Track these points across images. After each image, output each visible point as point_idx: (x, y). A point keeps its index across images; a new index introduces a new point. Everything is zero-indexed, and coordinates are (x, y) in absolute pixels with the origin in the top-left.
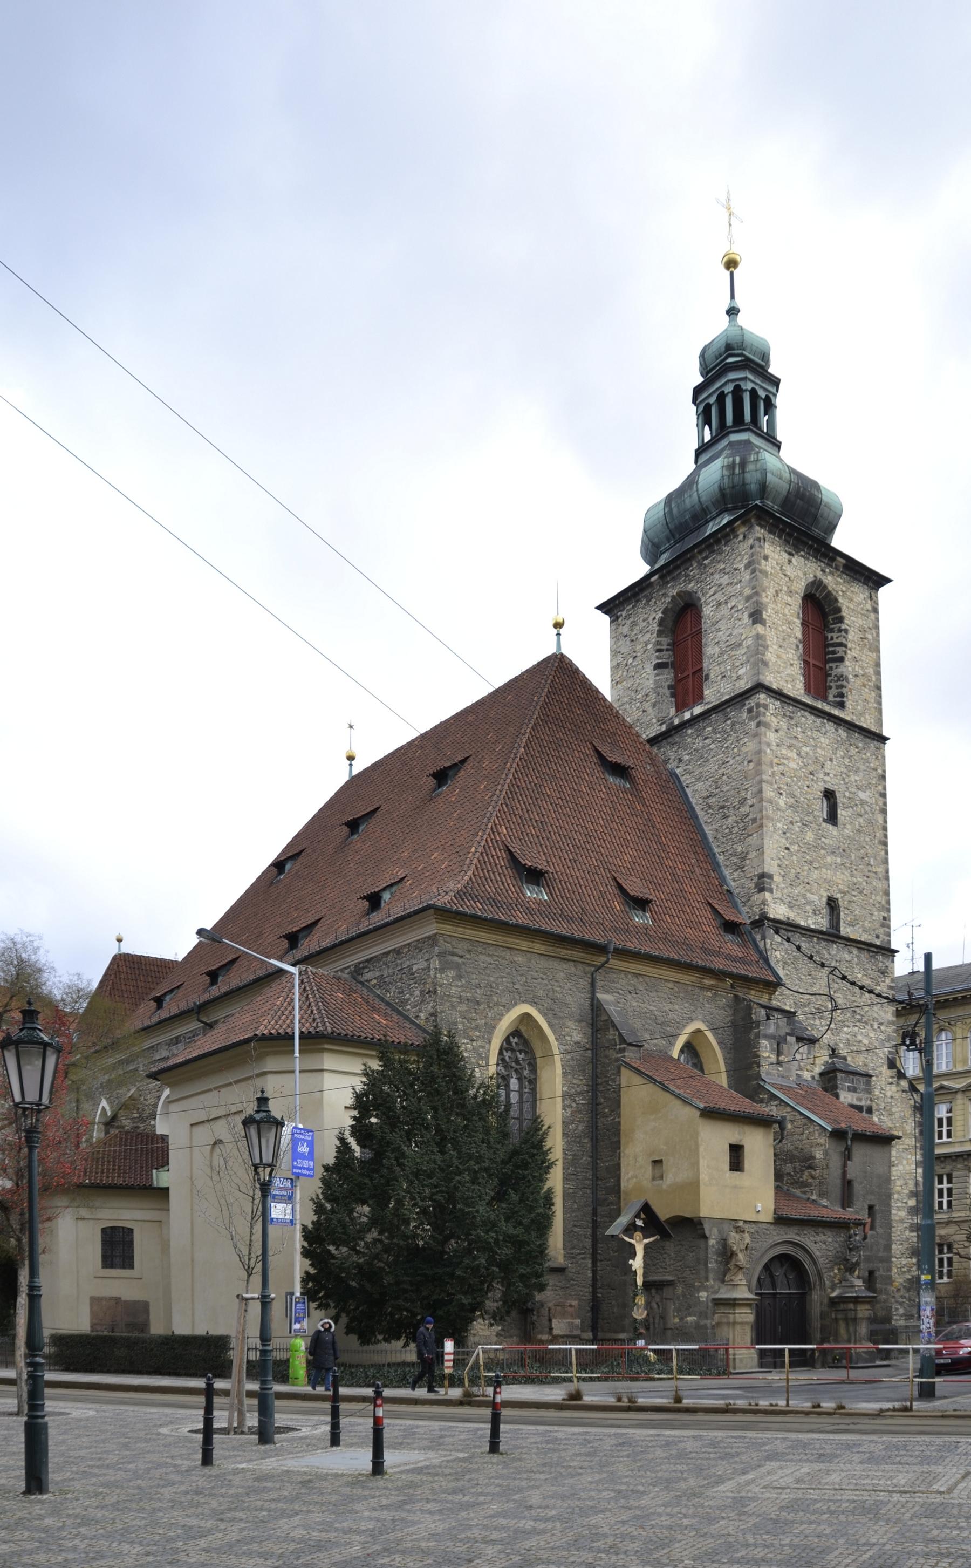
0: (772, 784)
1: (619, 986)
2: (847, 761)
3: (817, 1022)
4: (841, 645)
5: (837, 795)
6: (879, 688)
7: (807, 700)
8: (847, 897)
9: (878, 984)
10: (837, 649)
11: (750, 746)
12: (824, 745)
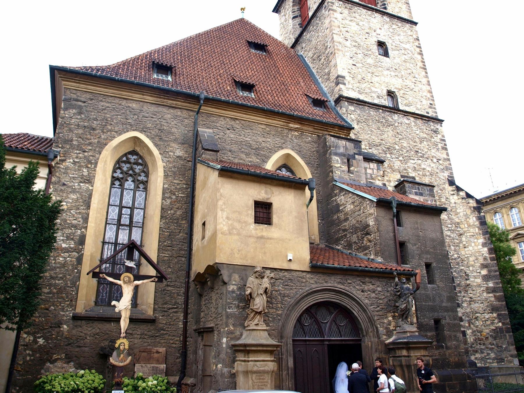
1: (218, 125)
2: (391, 30)
3: (388, 155)
5: (386, 43)
6: (408, 4)
7: (360, 2)
9: (432, 137)
11: (327, 21)
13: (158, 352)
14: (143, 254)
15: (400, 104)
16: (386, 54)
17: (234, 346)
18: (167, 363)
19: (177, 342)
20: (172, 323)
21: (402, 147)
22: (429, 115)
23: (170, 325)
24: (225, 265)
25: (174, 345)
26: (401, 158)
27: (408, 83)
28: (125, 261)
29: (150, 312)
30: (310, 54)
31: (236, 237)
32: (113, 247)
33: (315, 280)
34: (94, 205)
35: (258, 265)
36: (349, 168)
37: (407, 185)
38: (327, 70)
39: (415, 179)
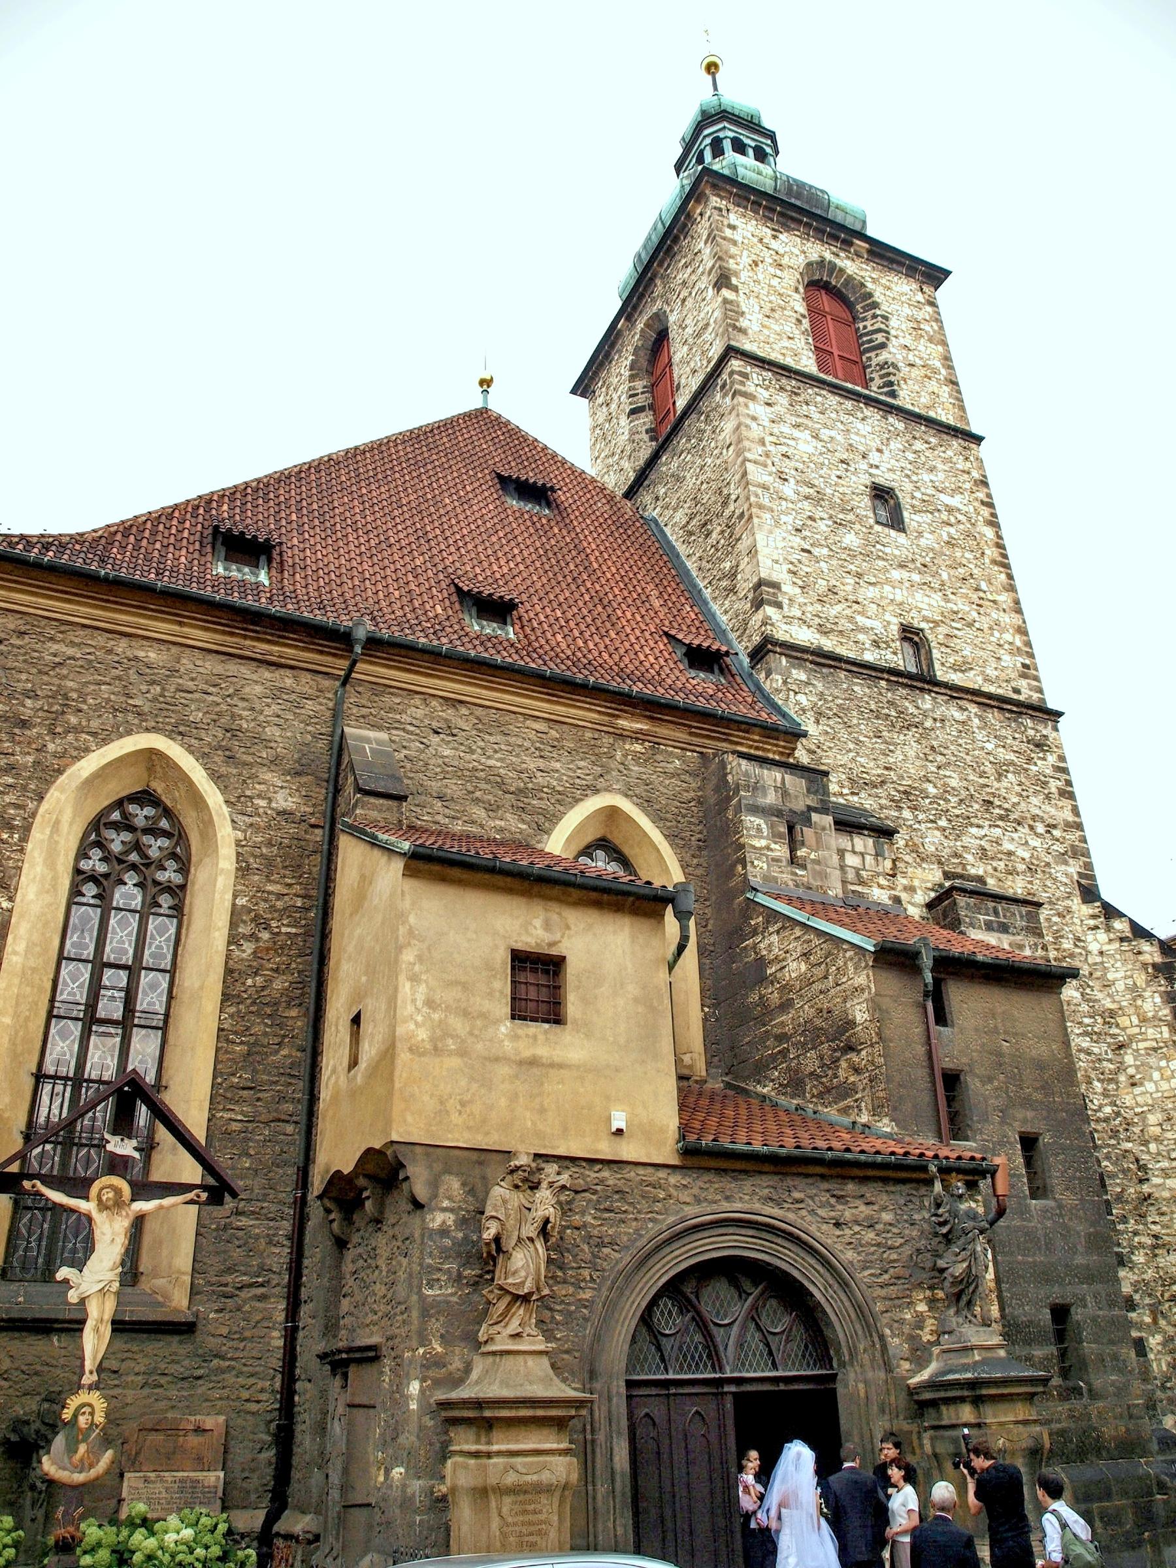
0: (766, 466)
1: (405, 718)
2: (911, 456)
3: (906, 814)
4: (879, 330)
7: (822, 375)
8: (943, 630)
9: (1029, 760)
10: (874, 336)
11: (728, 426)
12: (863, 432)
13: (199, 1430)
14: (162, 1114)
15: (937, 665)
16: (896, 522)
17: (445, 1405)
18: (229, 1464)
19: (264, 1397)
20: (247, 1334)
21: (947, 790)
22: (1022, 698)
23: (242, 1340)
24: (418, 1149)
25: (253, 1407)
26: (943, 823)
27: (961, 605)
28: (107, 1136)
29: (179, 1301)
30: (680, 517)
31: (455, 1062)
32: (69, 1089)
33: (696, 1191)
34: (15, 958)
35: (521, 1148)
36: (792, 850)
37: (962, 901)
38: (727, 565)
39: (985, 883)
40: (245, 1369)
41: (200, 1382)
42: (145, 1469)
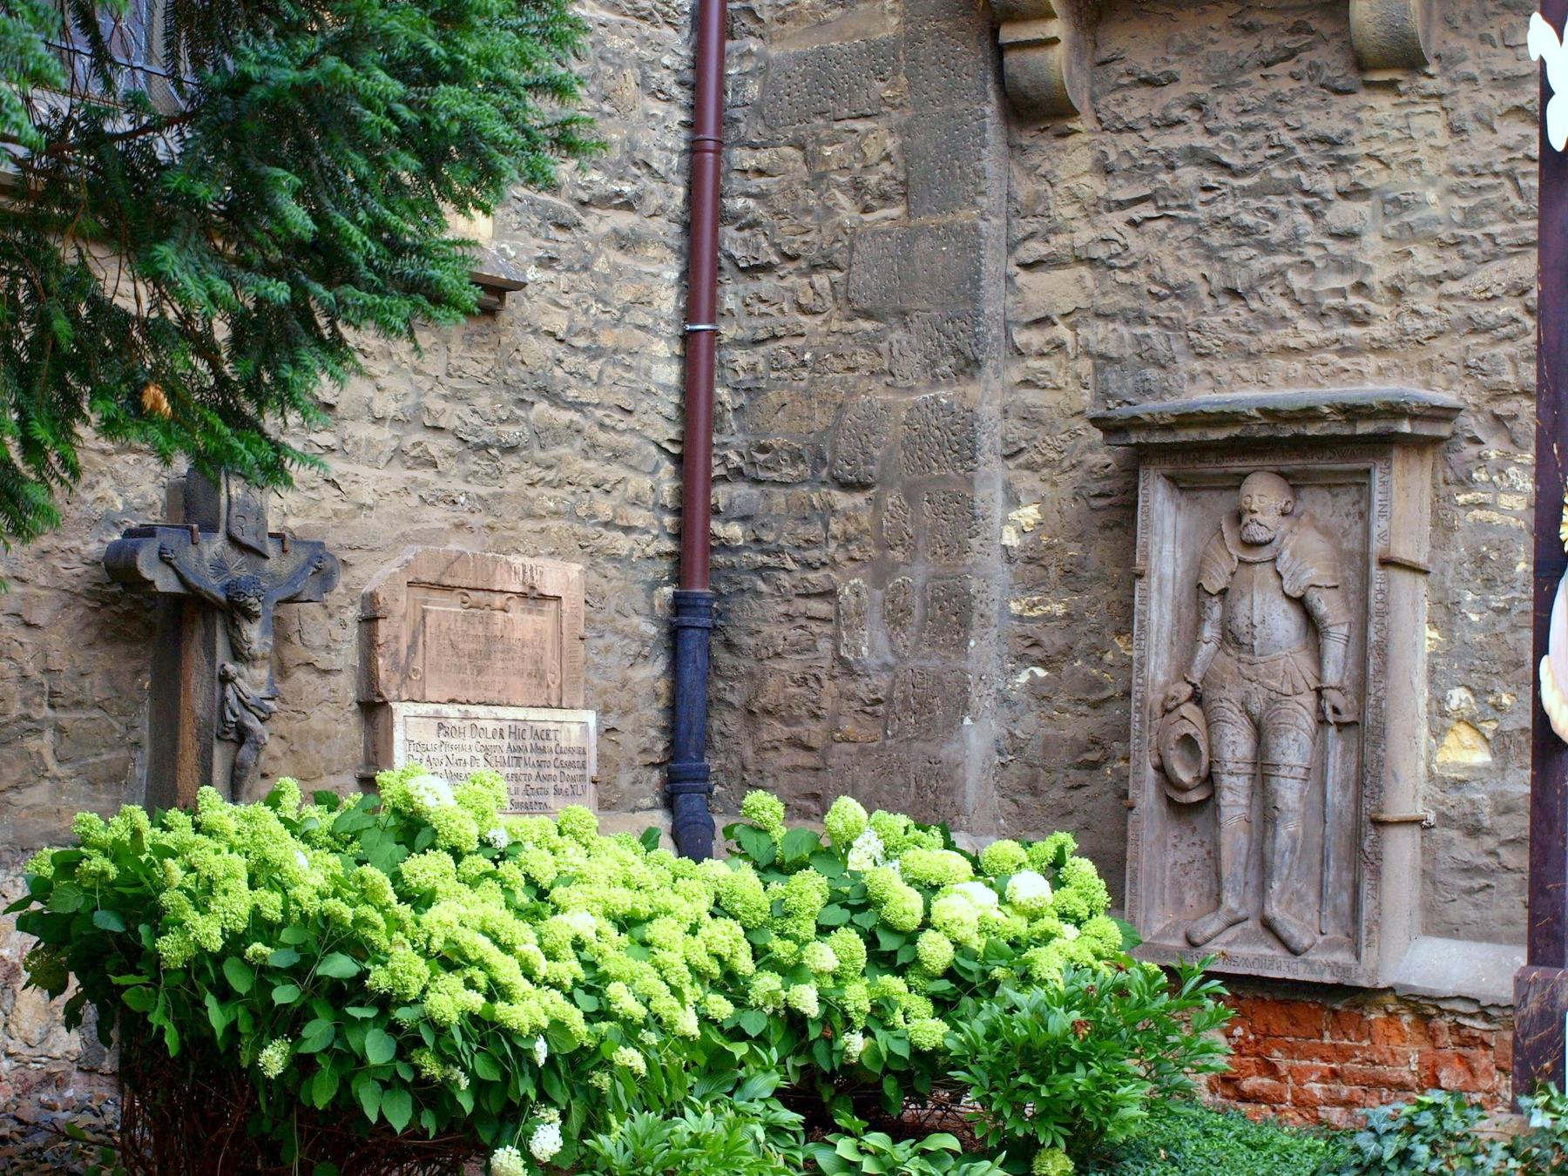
13: (534, 597)
20: (606, 340)
23: (594, 353)
25: (623, 543)
40: (602, 437)
41: (512, 461)
42: (430, 695)
